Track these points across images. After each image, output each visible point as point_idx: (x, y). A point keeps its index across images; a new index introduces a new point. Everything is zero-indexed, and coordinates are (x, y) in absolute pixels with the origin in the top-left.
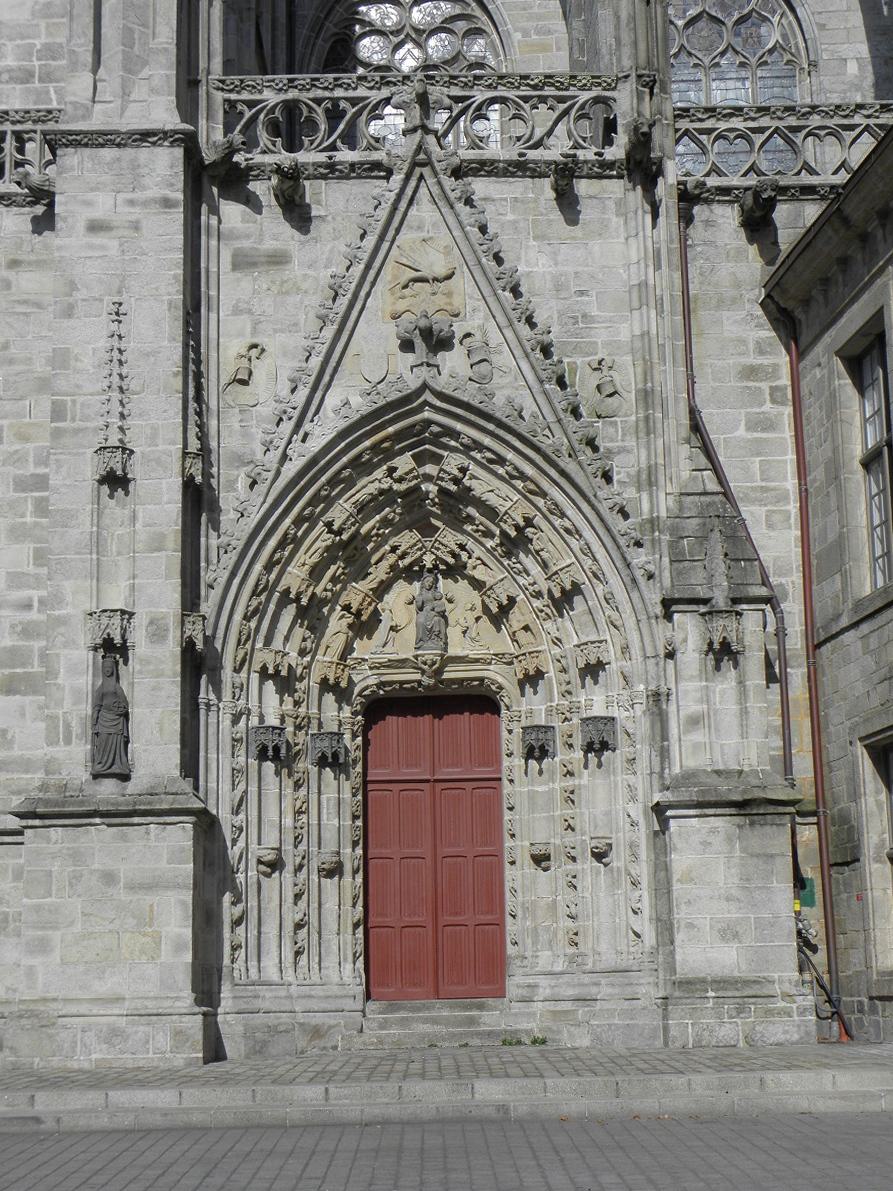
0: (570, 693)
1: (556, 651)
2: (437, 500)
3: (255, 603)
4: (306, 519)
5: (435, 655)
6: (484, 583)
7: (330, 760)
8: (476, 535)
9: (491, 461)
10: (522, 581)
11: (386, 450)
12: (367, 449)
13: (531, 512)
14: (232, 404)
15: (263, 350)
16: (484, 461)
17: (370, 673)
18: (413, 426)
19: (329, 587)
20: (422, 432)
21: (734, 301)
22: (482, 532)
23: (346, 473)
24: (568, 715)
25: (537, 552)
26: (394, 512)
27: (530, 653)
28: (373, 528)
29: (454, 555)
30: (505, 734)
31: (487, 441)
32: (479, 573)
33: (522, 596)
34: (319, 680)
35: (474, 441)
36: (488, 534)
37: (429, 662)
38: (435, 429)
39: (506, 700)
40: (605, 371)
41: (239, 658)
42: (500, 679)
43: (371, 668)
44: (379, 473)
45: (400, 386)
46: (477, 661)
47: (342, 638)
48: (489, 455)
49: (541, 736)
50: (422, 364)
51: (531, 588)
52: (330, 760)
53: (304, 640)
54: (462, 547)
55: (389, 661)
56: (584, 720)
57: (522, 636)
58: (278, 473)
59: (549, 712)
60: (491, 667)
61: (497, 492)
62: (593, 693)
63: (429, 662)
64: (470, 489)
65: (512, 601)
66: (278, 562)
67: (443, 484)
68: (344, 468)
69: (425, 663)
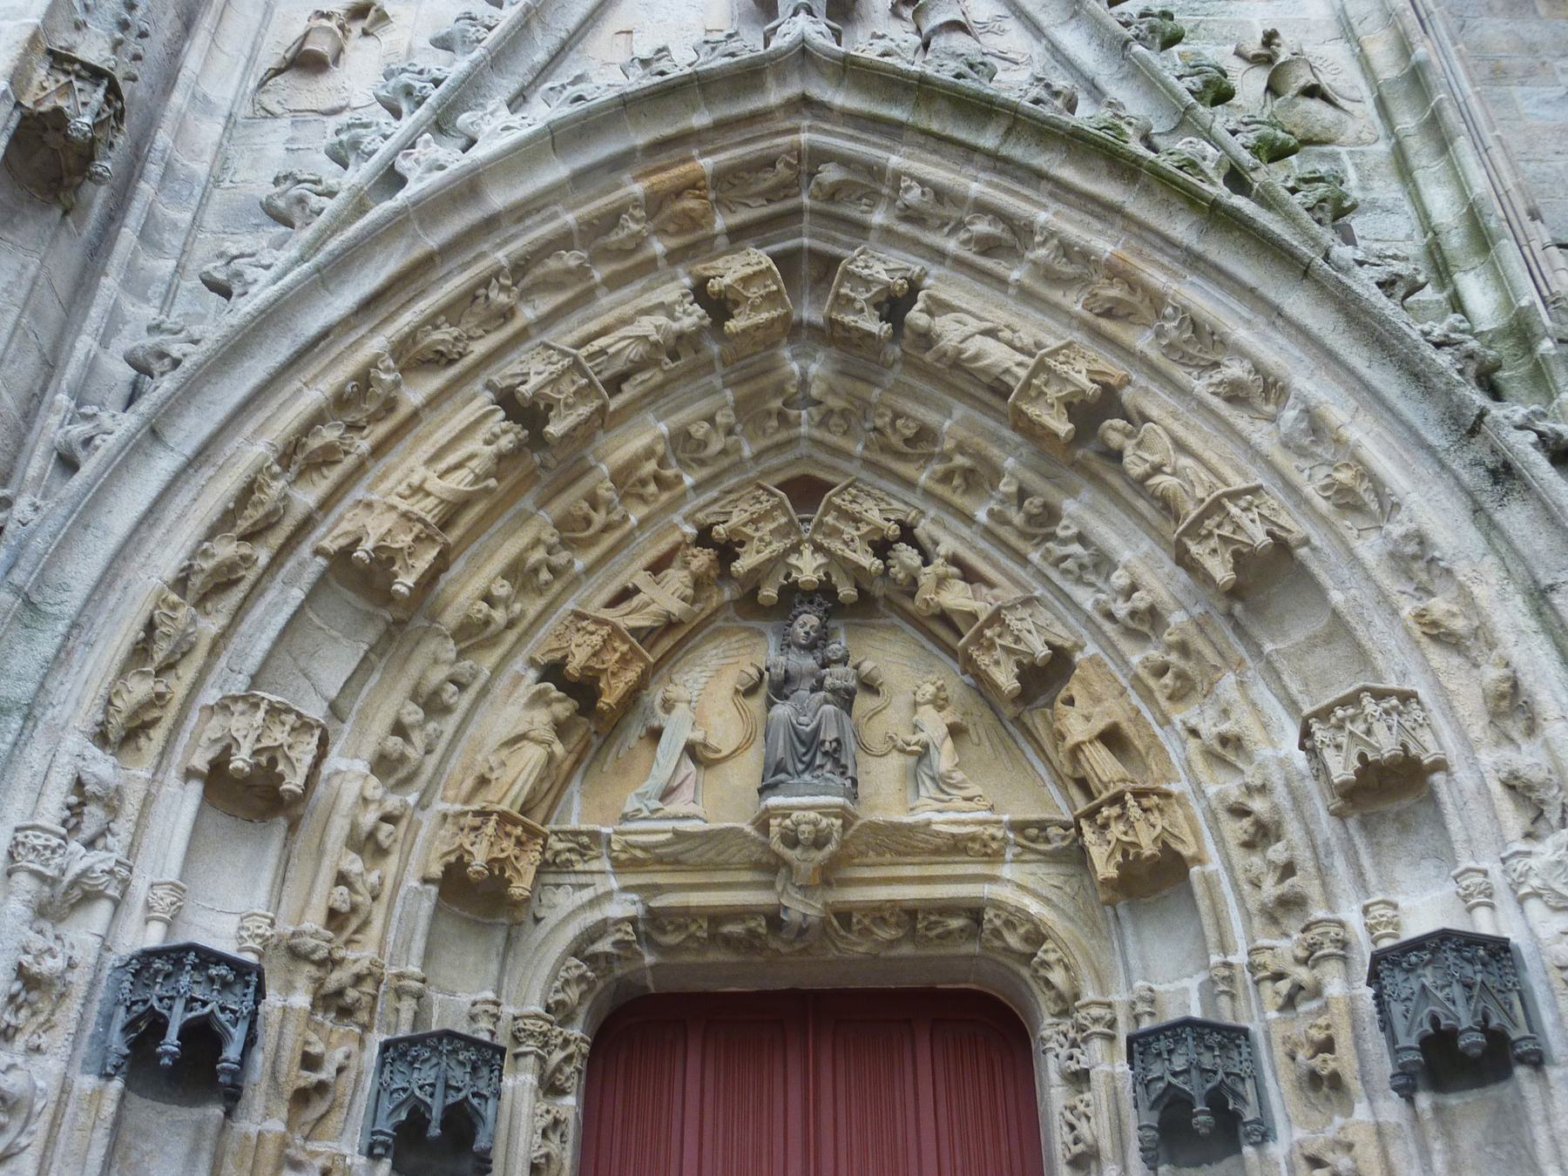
0: (1291, 903)
1: (1223, 786)
2: (835, 403)
3: (226, 550)
4: (440, 359)
5: (825, 811)
6: (973, 616)
7: (434, 1131)
8: (940, 489)
9: (988, 246)
10: (1085, 598)
11: (691, 222)
12: (635, 202)
13: (1115, 368)
14: (277, 109)
15: (383, 17)
16: (968, 254)
17: (614, 883)
18: (768, 162)
19: (502, 589)
20: (784, 189)
21: (1530, 72)
22: (968, 473)
23: (571, 259)
24: (1303, 974)
25: (1139, 484)
26: (711, 419)
27: (1139, 794)
28: (649, 453)
29: (882, 548)
30: (1055, 1096)
31: (976, 185)
32: (957, 597)
33: (1091, 649)
34: (436, 870)
35: (941, 194)
36: (978, 477)
37: (805, 831)
38: (830, 174)
39: (1057, 977)
40: (1284, 55)
41: (125, 703)
42: (1034, 907)
43: (619, 866)
44: (675, 289)
45: (733, 46)
46: (957, 846)
47: (533, 755)
48: (982, 227)
49: (1207, 1060)
50: (795, 13)
51: (1121, 609)
52: (434, 1131)
53: (399, 729)
54: (907, 533)
55: (679, 835)
56: (1386, 963)
57: (1104, 766)
58: (360, 209)
59: (1222, 983)
60: (1006, 871)
61: (1006, 334)
62: (1388, 882)
63: (805, 831)
64: (926, 339)
65: (1060, 664)
66: (327, 457)
67: (849, 319)
68: (563, 241)
69: (791, 840)
